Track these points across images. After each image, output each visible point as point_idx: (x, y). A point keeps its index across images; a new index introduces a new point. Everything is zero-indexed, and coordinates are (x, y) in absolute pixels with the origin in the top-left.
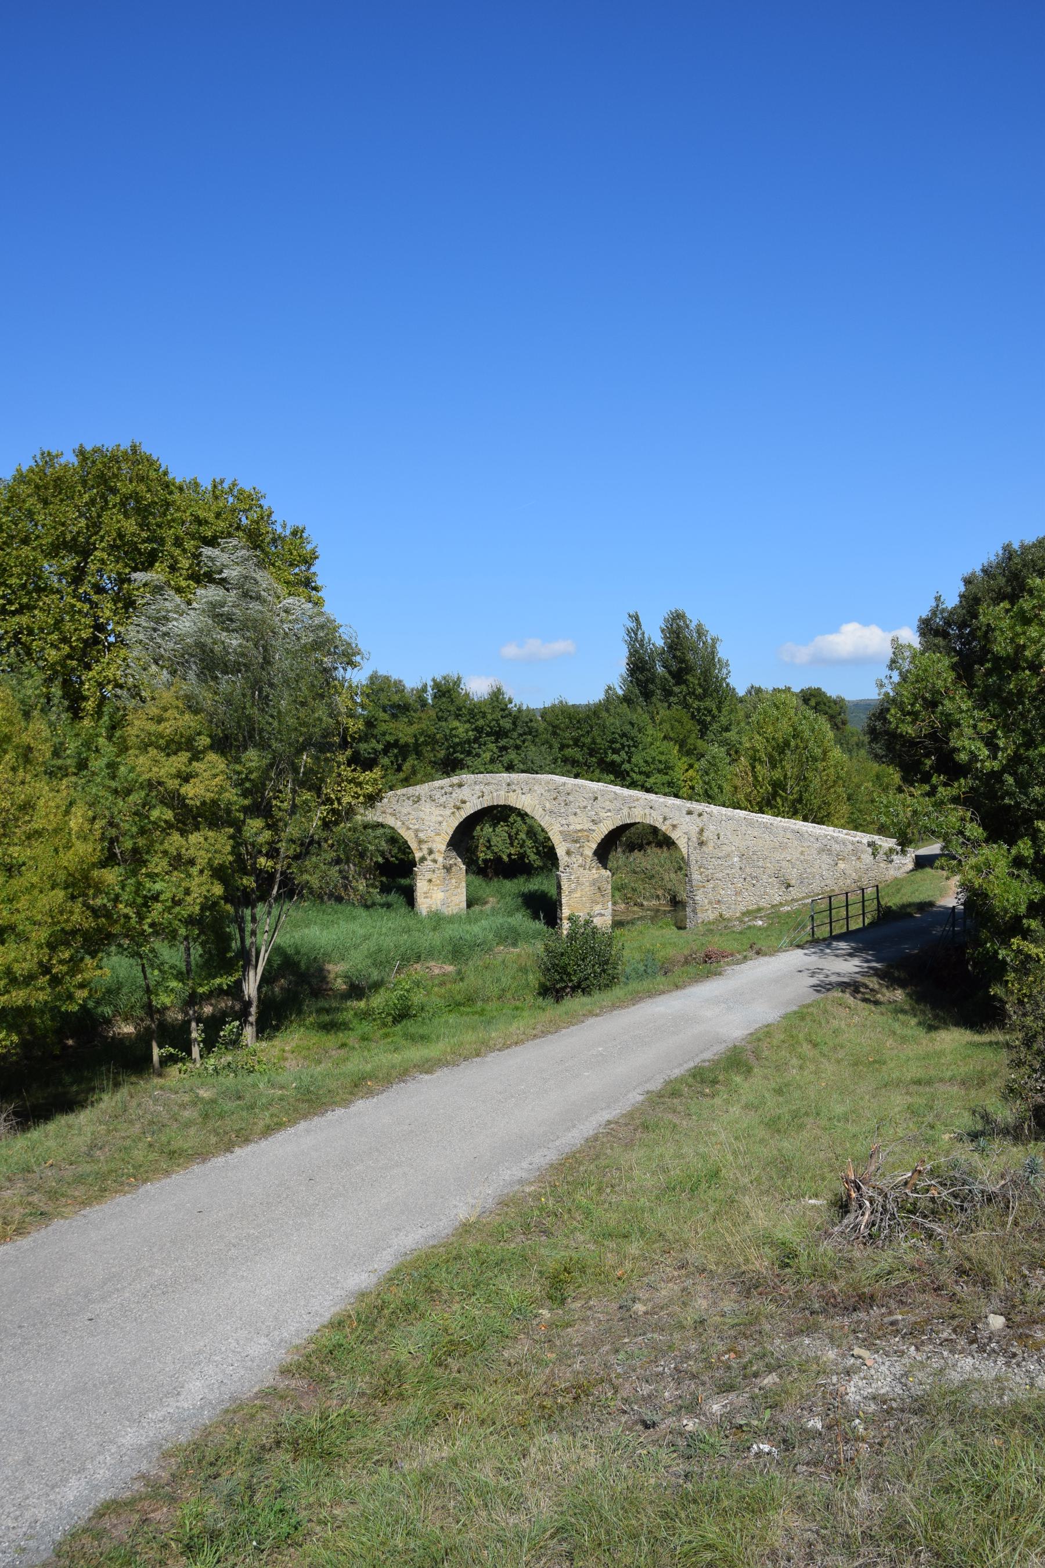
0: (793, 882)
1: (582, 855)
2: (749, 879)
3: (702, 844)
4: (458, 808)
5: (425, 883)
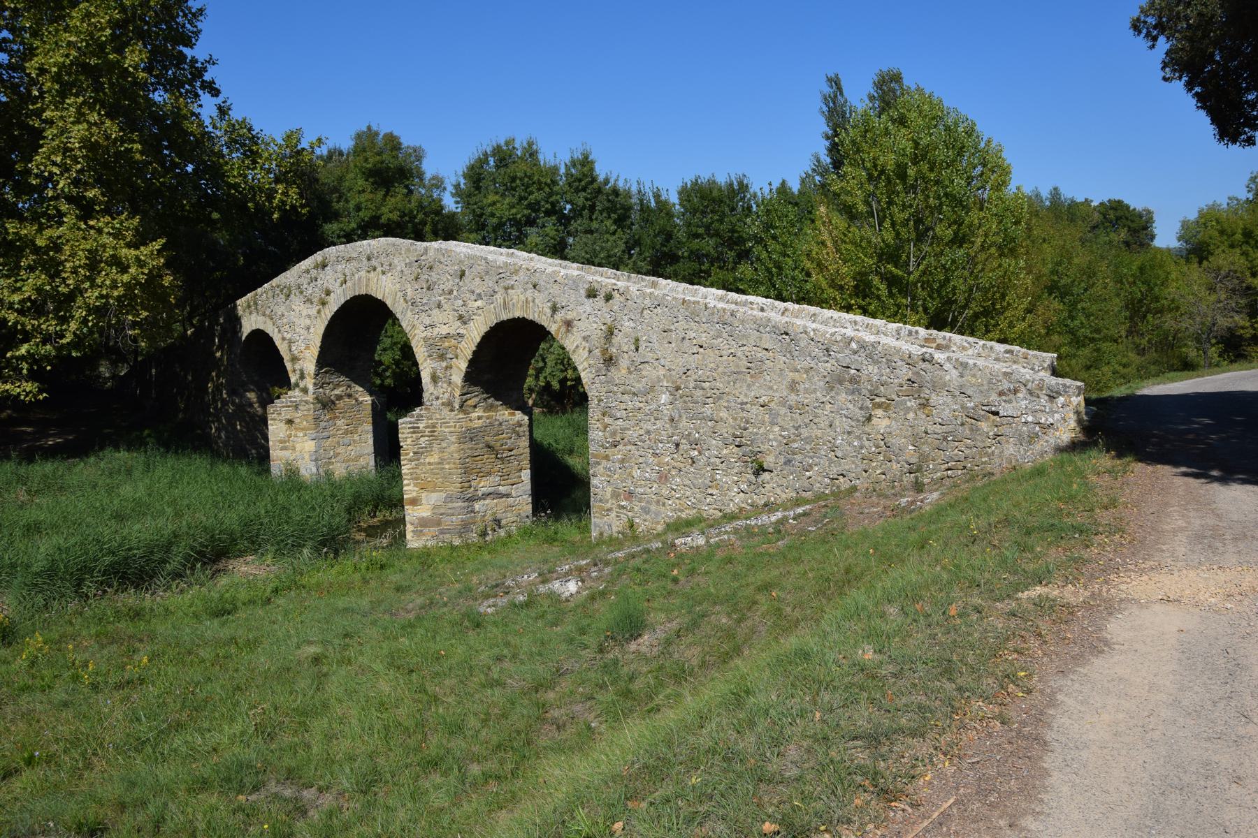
0: (769, 461)
2: (684, 446)
3: (609, 361)
4: (324, 303)
5: (283, 426)
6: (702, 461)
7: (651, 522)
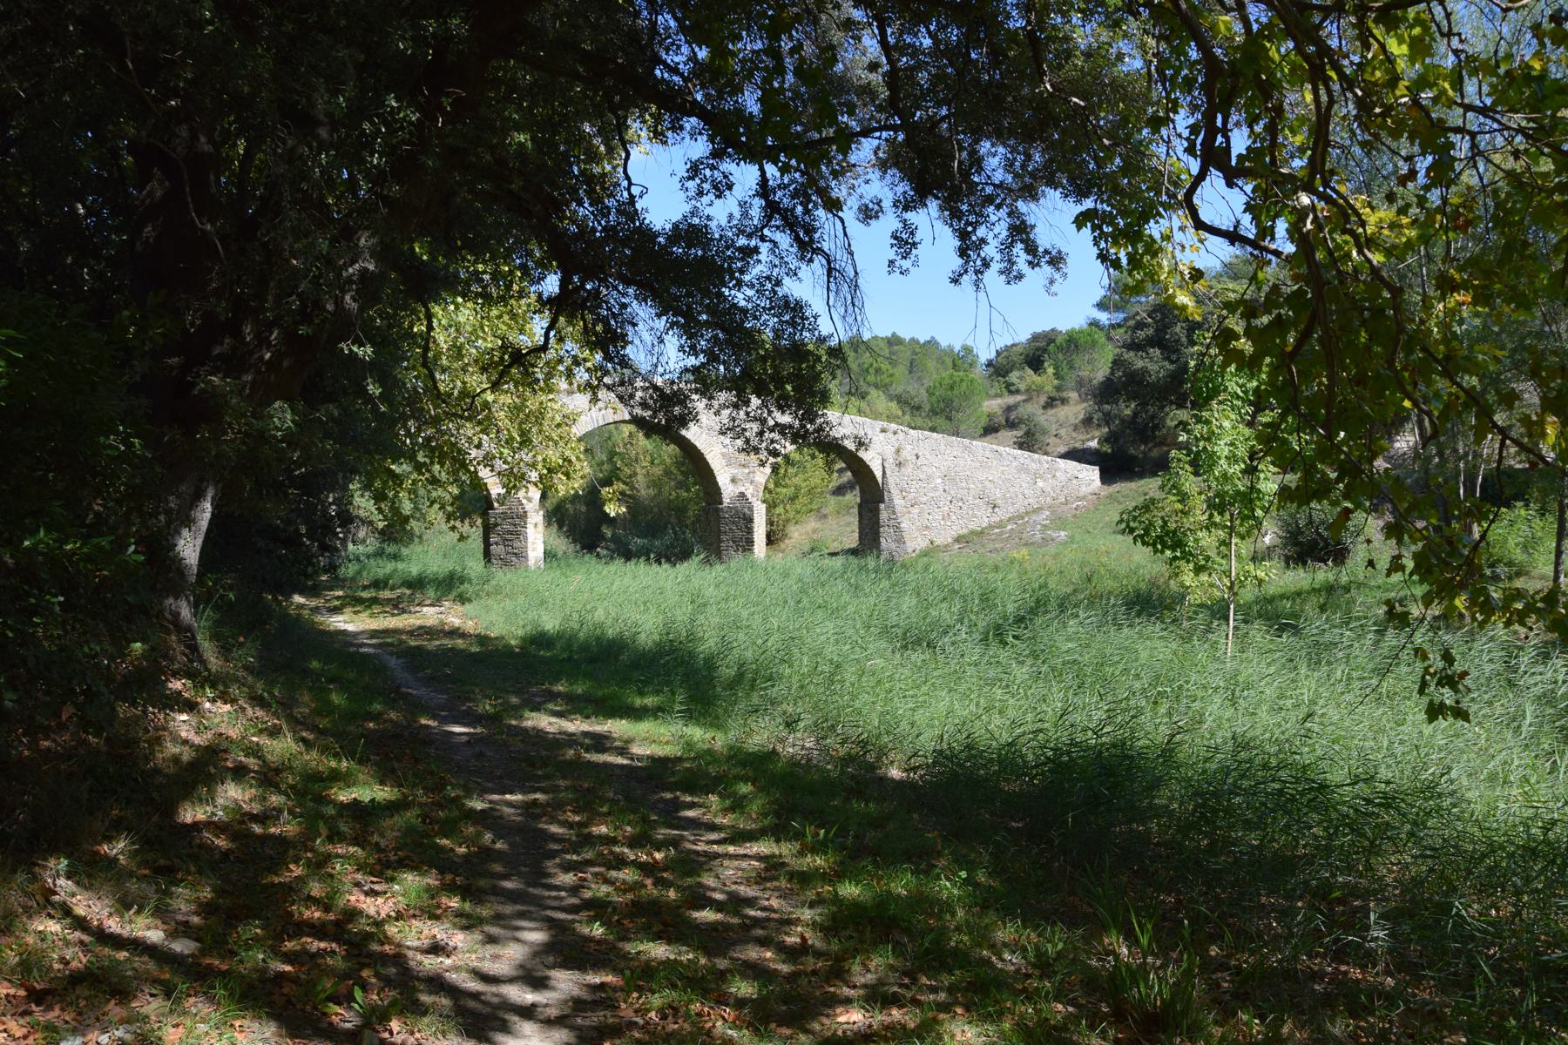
0: (999, 502)
1: (752, 482)
3: (899, 465)
7: (944, 537)
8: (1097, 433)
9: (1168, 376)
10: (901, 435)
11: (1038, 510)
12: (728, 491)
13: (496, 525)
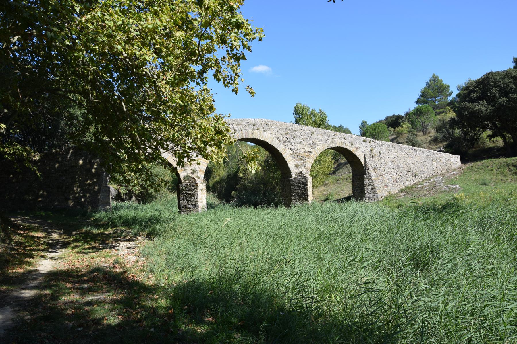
1: (305, 167)
3: (372, 157)
6: (403, 176)
7: (395, 190)
8: (441, 145)
9: (491, 112)
10: (372, 143)
11: (436, 176)
12: (294, 172)
13: (183, 191)
